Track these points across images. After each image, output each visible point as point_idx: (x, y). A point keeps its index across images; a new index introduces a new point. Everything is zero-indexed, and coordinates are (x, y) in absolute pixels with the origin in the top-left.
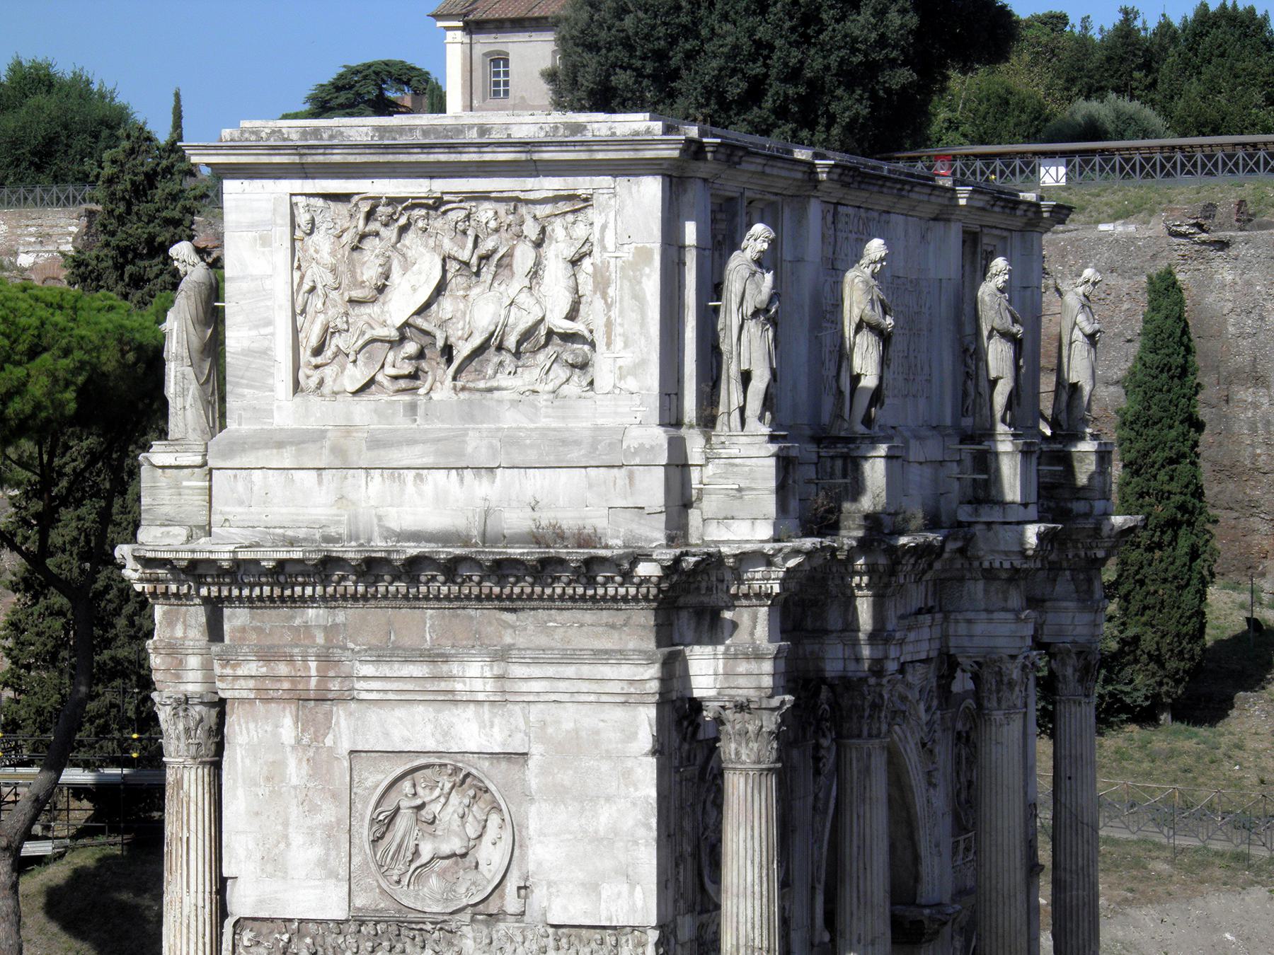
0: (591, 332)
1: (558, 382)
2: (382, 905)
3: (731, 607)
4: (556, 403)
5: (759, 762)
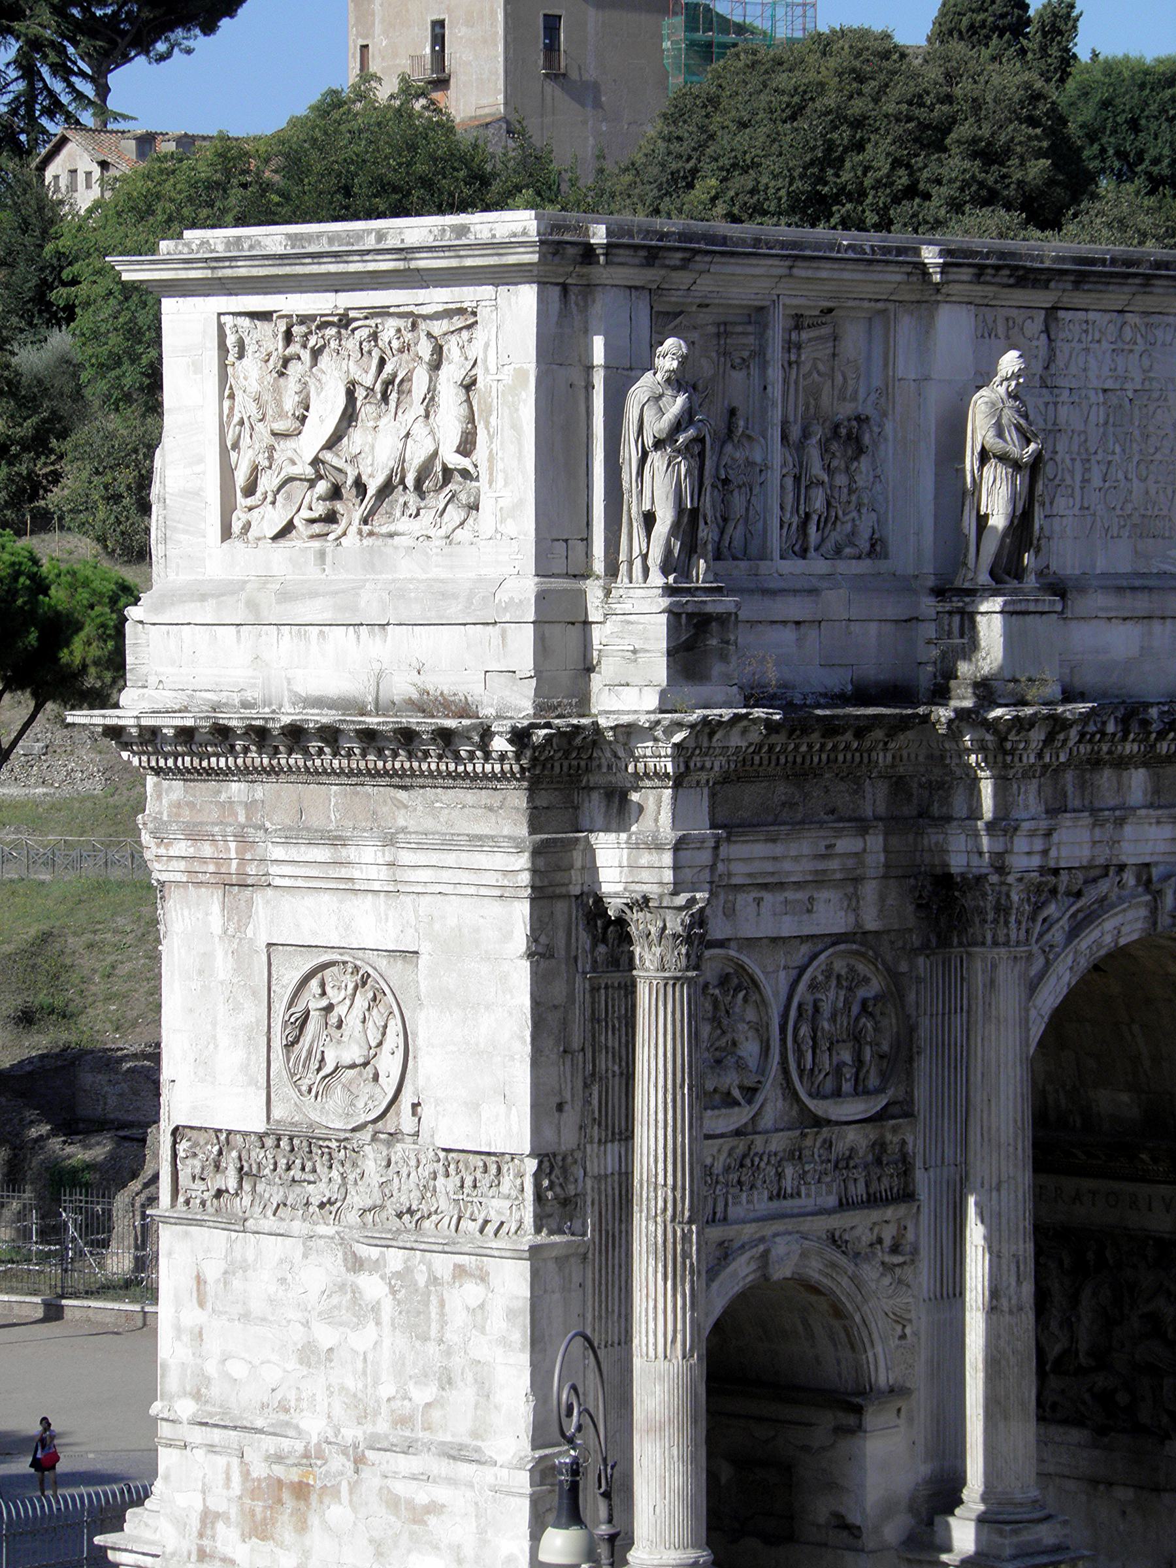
0: (476, 466)
1: (451, 526)
2: (296, 1118)
3: (637, 789)
4: (447, 550)
5: (663, 969)
